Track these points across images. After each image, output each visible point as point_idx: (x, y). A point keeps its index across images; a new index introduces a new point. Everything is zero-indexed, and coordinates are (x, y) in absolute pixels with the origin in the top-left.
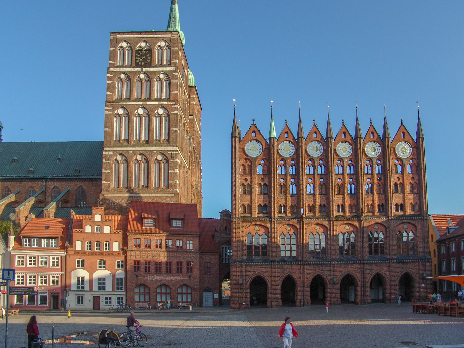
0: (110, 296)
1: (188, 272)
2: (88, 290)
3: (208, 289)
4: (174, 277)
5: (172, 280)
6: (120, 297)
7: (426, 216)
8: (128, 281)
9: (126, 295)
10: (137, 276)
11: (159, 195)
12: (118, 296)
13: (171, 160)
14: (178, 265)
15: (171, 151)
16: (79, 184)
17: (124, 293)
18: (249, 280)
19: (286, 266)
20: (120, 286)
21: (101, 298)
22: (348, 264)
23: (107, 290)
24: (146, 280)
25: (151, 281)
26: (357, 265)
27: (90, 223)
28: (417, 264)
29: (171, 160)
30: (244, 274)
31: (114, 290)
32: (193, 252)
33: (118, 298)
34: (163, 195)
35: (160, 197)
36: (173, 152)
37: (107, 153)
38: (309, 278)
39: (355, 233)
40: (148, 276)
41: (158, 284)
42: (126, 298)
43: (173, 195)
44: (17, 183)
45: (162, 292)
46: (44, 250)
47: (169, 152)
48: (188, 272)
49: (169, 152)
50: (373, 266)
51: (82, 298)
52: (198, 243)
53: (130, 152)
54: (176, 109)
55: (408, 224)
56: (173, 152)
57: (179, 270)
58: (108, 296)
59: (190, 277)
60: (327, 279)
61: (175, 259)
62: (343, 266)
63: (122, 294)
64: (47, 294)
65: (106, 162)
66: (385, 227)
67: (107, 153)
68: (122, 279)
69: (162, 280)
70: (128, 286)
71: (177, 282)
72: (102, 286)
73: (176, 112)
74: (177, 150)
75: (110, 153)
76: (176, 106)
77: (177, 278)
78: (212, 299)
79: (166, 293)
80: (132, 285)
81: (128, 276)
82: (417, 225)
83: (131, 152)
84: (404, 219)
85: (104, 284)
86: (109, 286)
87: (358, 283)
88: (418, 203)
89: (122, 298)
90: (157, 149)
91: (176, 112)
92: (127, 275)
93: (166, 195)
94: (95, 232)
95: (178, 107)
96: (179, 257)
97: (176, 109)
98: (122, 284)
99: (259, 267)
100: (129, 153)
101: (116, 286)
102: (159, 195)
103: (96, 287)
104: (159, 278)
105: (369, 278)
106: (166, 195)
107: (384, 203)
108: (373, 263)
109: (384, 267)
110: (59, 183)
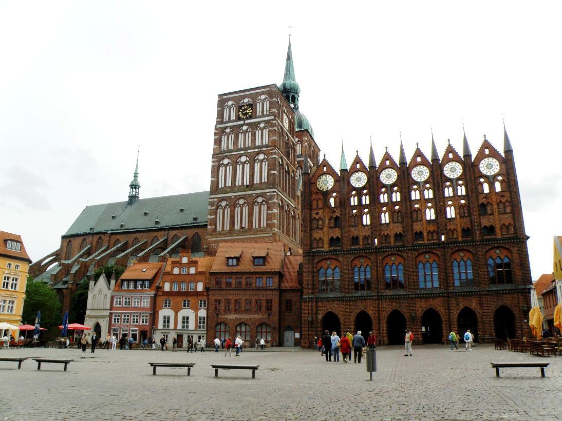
0: (167, 334)
1: (268, 310)
2: (173, 328)
3: (289, 328)
4: (253, 316)
5: (251, 319)
7: (523, 238)
10: (217, 315)
11: (257, 236)
12: (200, 335)
14: (268, 303)
15: (269, 192)
16: (195, 230)
18: (320, 317)
19: (359, 301)
21: (184, 337)
22: (430, 297)
23: (190, 328)
24: (226, 318)
25: (231, 320)
26: (441, 299)
27: (178, 265)
28: (516, 295)
30: (314, 310)
32: (272, 290)
34: (261, 235)
35: (259, 237)
37: (213, 200)
38: (385, 315)
39: (437, 262)
40: (227, 315)
41: (238, 323)
43: (271, 235)
44: (145, 234)
45: (242, 330)
46: (132, 291)
47: (268, 194)
48: (268, 310)
49: (268, 194)
50: (460, 299)
52: (278, 280)
54: (275, 153)
55: (500, 249)
57: (259, 310)
59: (269, 315)
60: (407, 316)
61: (255, 297)
62: (423, 300)
64: (137, 333)
65: (212, 208)
66: (472, 253)
67: (213, 200)
68: (204, 318)
69: (241, 319)
71: (256, 320)
73: (274, 156)
74: (275, 192)
75: (215, 200)
76: (274, 151)
77: (256, 316)
78: (293, 338)
79: (245, 332)
82: (512, 249)
84: (495, 243)
85: (187, 322)
86: (192, 326)
87: (443, 319)
88: (512, 223)
91: (274, 156)
93: (264, 235)
94: (182, 273)
95: (277, 151)
96: (259, 295)
97: (275, 153)
98: (204, 323)
99: (331, 302)
101: (198, 325)
102: (257, 236)
103: (180, 326)
104: (238, 316)
105: (455, 314)
106: (264, 235)
107: (469, 226)
108: (459, 296)
109: (474, 300)
110: (178, 231)
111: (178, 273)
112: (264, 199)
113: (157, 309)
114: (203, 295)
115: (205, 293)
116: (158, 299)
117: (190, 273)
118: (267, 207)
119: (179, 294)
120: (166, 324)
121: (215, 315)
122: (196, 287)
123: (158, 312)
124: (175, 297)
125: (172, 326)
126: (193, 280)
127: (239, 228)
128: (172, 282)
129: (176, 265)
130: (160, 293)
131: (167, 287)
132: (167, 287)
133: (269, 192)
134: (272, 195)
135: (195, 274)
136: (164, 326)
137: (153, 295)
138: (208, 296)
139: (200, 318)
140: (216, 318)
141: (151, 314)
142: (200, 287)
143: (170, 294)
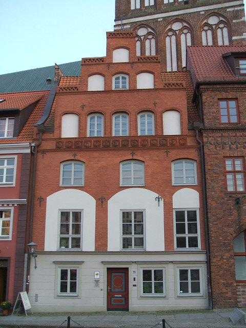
2: (93, 249)
6: (189, 268)
8: (212, 219)
9: (209, 263)
13: (234, 21)
15: (232, 7)
17: (202, 258)
20: (187, 235)
21: (131, 275)
29: (234, 21)
31: (168, 251)
33: (183, 273)
36: (236, 9)
37: (120, 28)
42: (209, 272)
51: (74, 274)
53: (159, 20)
56: (236, 9)
58: (153, 268)
63: (195, 258)
70: (212, 234)
72: (133, 236)
75: (125, 27)
80: (226, 229)
81: (212, 203)
83: (162, 19)
89: (195, 273)
90: (207, 9)
92: (209, 201)
98: (193, 229)
100: (157, 21)
103: (115, 241)
111: (102, 89)
112: (221, 19)
113: (39, 193)
114: (183, 146)
115: (190, 142)
116: (43, 161)
117: (139, 87)
118: (229, 32)
119: (108, 144)
120: (71, 235)
121: (231, 203)
122: (159, 125)
123: (43, 201)
124: (96, 154)
125: (88, 241)
126: (151, 107)
127: (175, 69)
128: (83, 115)
129: (95, 69)
130: (49, 145)
131: (69, 127)
132: (69, 127)
133: (232, 7)
134: (238, 11)
135: (155, 89)
136: (64, 241)
137: (28, 151)
138: (200, 148)
139: (180, 215)
140: (235, 212)
141: (21, 206)
142: (172, 124)
143: (78, 146)
